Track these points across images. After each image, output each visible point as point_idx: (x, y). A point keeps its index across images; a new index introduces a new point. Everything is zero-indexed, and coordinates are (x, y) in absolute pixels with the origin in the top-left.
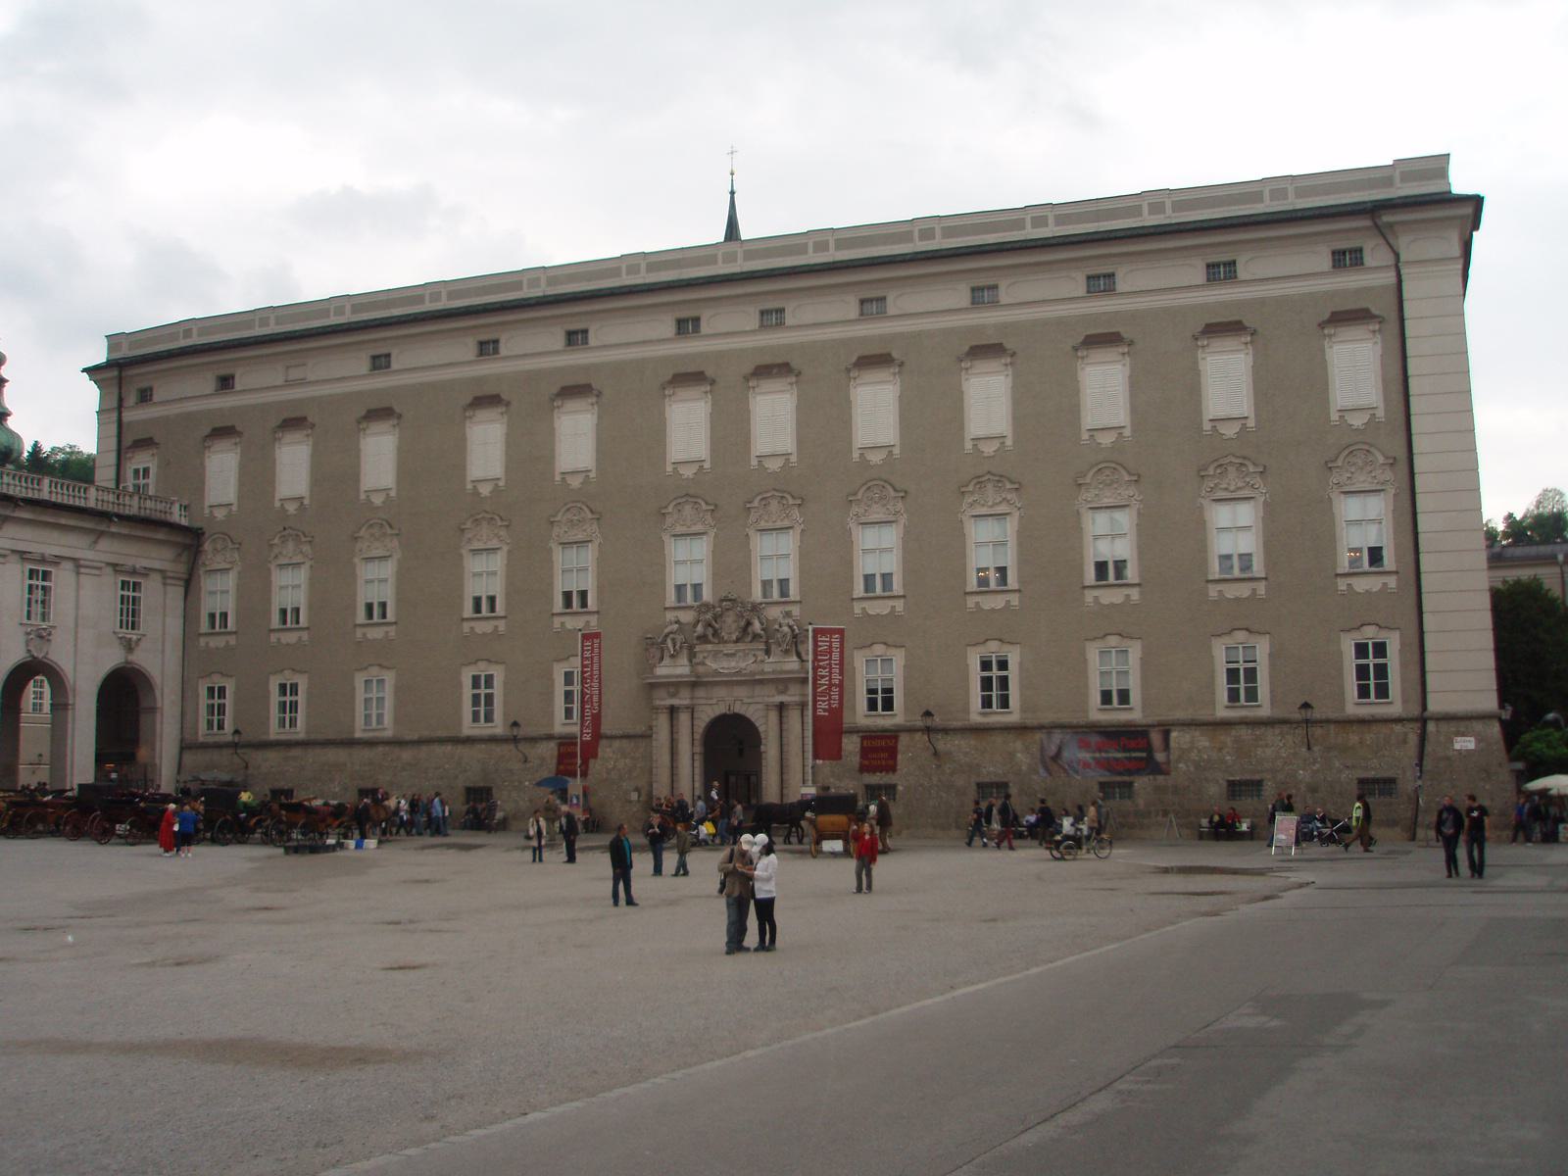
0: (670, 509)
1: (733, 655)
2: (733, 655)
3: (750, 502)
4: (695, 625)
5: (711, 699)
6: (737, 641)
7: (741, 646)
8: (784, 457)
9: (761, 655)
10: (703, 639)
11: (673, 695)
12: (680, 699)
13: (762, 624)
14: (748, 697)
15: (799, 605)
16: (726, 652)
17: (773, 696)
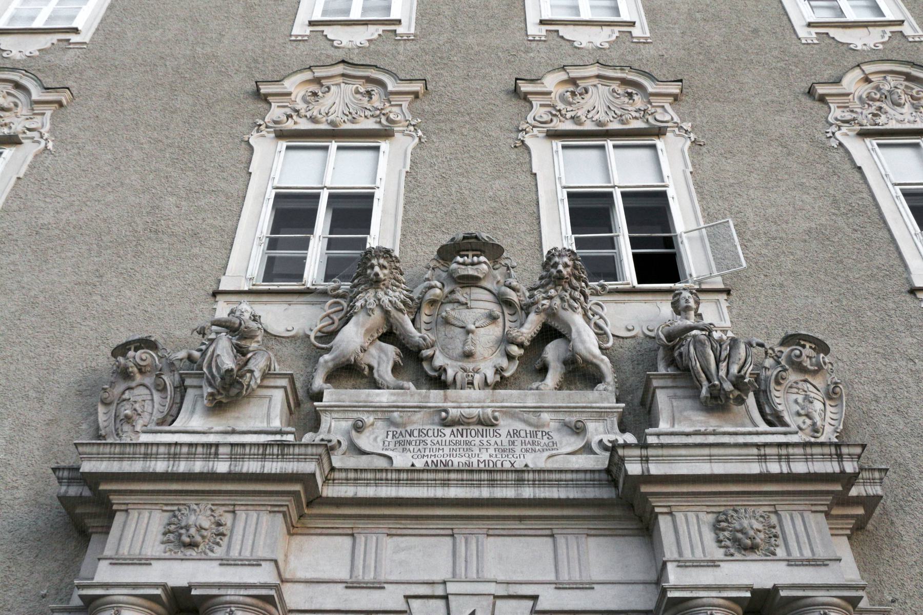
0: (289, 85)
1: (486, 423)
2: (486, 423)
3: (532, 81)
4: (328, 336)
5: (378, 586)
6: (503, 382)
7: (511, 397)
8: (617, 29)
9: (601, 432)
10: (350, 372)
11: (182, 542)
12: (225, 562)
13: (601, 334)
14: (559, 586)
15: (722, 297)
16: (454, 413)
17: (713, 564)
